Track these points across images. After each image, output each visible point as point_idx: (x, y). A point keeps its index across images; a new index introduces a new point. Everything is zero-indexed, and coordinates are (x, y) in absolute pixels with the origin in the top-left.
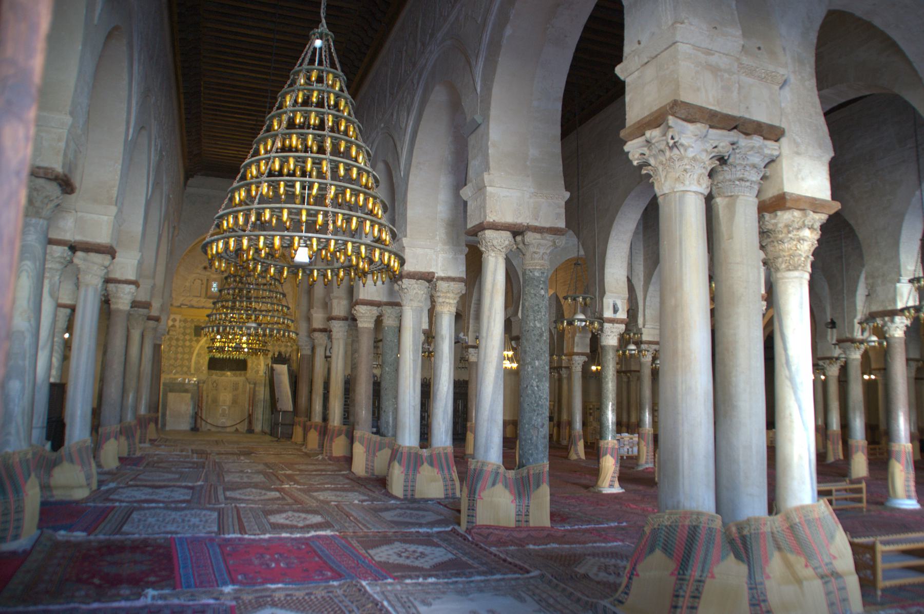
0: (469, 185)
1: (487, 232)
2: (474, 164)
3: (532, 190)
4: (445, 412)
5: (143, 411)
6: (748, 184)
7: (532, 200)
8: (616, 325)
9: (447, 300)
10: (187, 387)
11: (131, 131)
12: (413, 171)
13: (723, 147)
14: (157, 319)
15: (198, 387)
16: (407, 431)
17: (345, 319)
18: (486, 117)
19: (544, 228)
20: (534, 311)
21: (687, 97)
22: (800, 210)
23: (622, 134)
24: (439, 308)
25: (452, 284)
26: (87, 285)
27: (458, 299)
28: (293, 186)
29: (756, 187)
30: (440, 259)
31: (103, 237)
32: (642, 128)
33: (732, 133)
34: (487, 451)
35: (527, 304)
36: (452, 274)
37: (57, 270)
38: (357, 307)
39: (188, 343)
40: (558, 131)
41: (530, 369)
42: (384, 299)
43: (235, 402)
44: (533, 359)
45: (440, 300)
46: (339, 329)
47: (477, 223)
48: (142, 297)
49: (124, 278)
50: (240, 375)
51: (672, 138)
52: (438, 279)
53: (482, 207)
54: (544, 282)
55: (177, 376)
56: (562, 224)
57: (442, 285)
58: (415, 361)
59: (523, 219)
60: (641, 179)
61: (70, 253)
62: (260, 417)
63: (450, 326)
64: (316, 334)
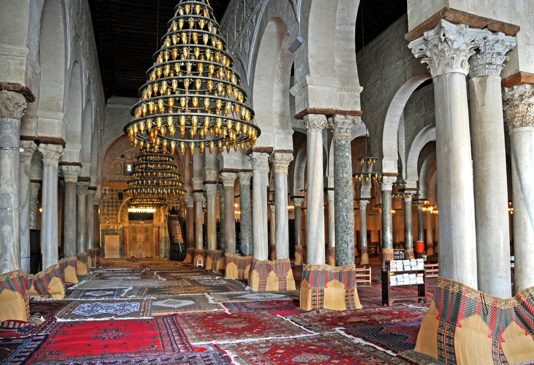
6: (495, 67)
7: (338, 93)
8: (391, 177)
9: (282, 165)
10: (116, 231)
13: (478, 41)
14: (95, 189)
15: (123, 231)
17: (214, 182)
19: (347, 111)
20: (342, 167)
21: (452, 5)
22: (530, 84)
24: (277, 171)
25: (284, 154)
26: (49, 165)
29: (500, 69)
30: (276, 139)
31: (57, 134)
32: (420, 31)
33: (484, 30)
34: (315, 259)
35: (337, 162)
38: (222, 174)
39: (115, 204)
40: (353, 46)
42: (240, 168)
43: (146, 239)
44: (342, 198)
45: (277, 165)
46: (211, 189)
48: (85, 174)
49: (72, 161)
50: (149, 223)
51: (444, 35)
53: (306, 99)
55: (110, 224)
56: (358, 109)
57: (278, 155)
60: (420, 68)
61: (35, 145)
62: (163, 248)
64: (197, 194)
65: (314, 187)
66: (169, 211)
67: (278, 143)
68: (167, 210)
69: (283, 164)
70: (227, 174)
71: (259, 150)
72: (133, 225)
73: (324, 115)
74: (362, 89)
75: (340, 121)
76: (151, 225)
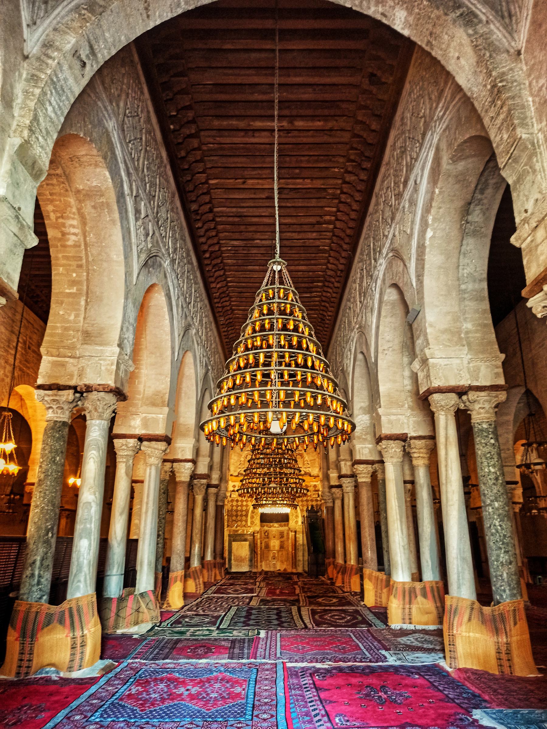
1: (434, 395)
2: (419, 342)
5: (209, 557)
10: (246, 537)
11: (176, 354)
14: (216, 486)
18: (422, 305)
19: (485, 387)
20: (487, 458)
23: (524, 293)
25: (423, 441)
28: (255, 376)
30: (411, 422)
31: (160, 430)
36: (421, 433)
37: (131, 456)
38: (356, 466)
41: (491, 510)
43: (282, 547)
48: (202, 469)
52: (411, 438)
53: (428, 376)
54: (493, 432)
56: (501, 381)
58: (399, 507)
59: (465, 381)
62: (301, 558)
64: (334, 490)
66: (307, 510)
68: (305, 508)
70: (362, 466)
71: (390, 438)
72: (266, 528)
74: (503, 356)
76: (287, 528)
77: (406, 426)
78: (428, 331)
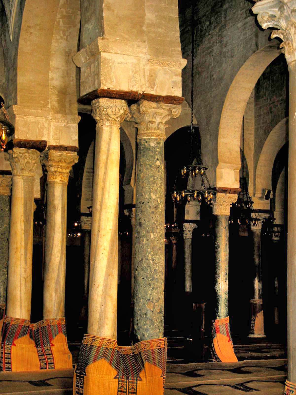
0: (82, 50)
3: (149, 57)
4: (57, 282)
9: (60, 170)
12: (23, 34)
16: (18, 303)
19: (160, 97)
24: (50, 179)
25: (64, 153)
27: (71, 168)
45: (52, 169)
47: (91, 90)
53: (97, 74)
54: (160, 153)
56: (178, 93)
58: (26, 231)
59: (139, 87)
63: (63, 196)
65: (103, 213)
67: (55, 134)
69: (61, 167)
73: (123, 101)
74: (184, 62)
75: (149, 110)
77: (45, 132)
78: (104, 15)
